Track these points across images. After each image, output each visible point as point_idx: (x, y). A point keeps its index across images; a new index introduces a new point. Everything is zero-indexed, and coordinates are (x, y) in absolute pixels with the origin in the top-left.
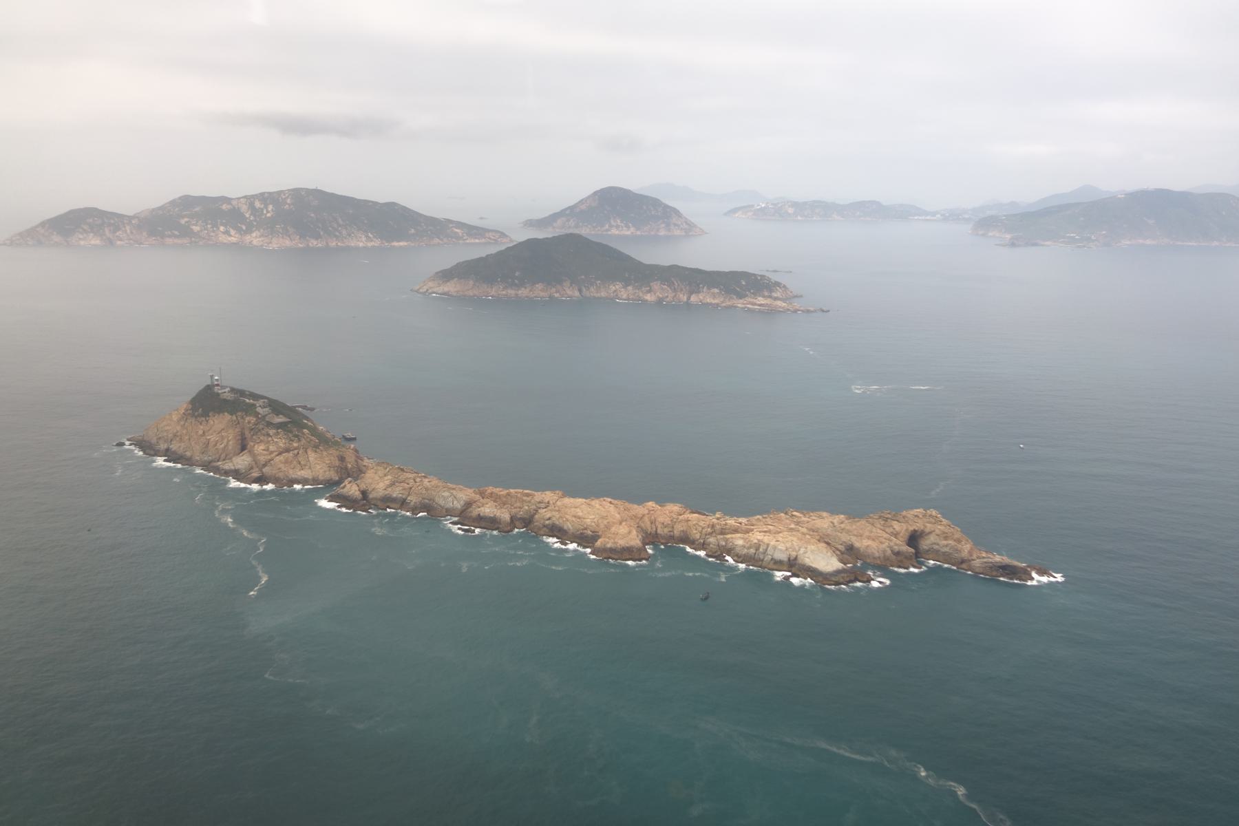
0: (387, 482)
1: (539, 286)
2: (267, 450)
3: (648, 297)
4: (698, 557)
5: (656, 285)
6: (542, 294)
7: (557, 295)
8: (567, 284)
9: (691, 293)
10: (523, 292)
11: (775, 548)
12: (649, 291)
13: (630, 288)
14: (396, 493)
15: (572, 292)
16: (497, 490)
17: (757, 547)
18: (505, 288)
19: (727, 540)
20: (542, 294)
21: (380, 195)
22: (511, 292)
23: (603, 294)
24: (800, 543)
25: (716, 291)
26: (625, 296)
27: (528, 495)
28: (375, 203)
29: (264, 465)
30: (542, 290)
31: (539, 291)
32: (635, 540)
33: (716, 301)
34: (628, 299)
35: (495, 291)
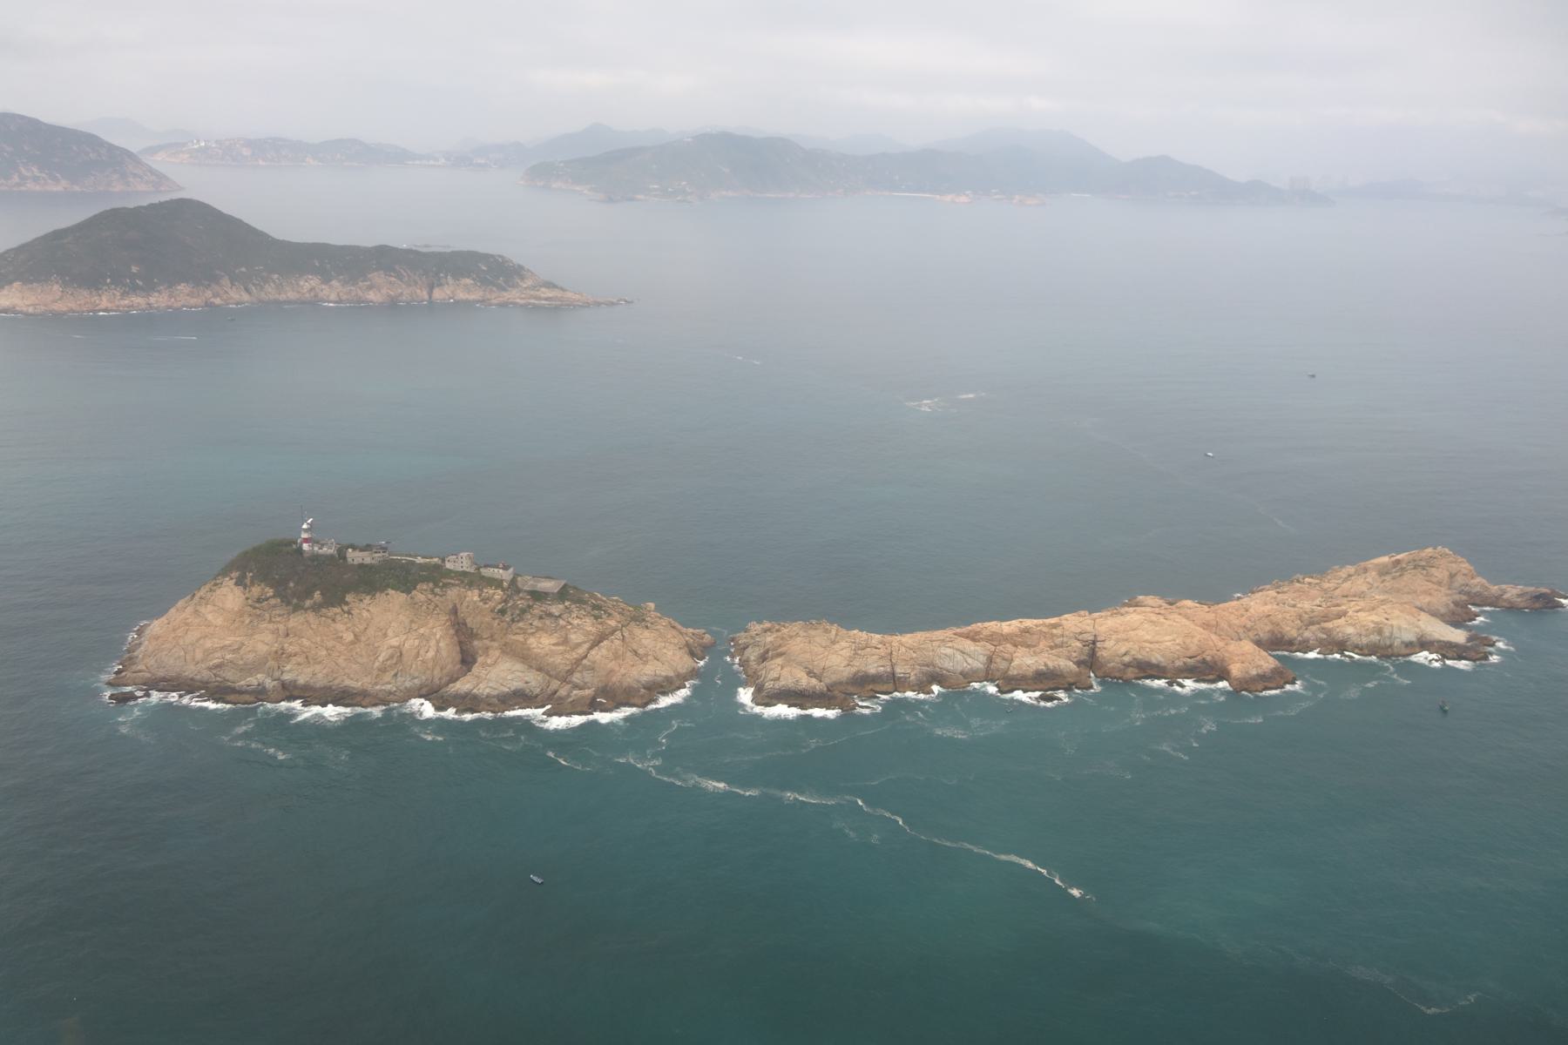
0: (847, 653)
1: (183, 288)
2: (565, 641)
3: (371, 295)
4: (1371, 664)
5: (378, 277)
6: (193, 301)
7: (218, 301)
8: (226, 281)
9: (431, 288)
10: (159, 300)
11: (1400, 628)
12: (370, 288)
13: (334, 283)
14: (873, 666)
15: (237, 296)
16: (993, 626)
17: (1380, 632)
18: (124, 295)
19: (1323, 630)
20: (193, 301)
21: (368, 240)
22: (138, 300)
23: (292, 295)
24: (1391, 609)
25: (468, 281)
26: (333, 297)
27: (1055, 626)
28: (290, 244)
29: (571, 672)
30: (191, 295)
31: (184, 297)
32: (1266, 662)
33: (472, 297)
34: (340, 301)
35: (107, 301)
